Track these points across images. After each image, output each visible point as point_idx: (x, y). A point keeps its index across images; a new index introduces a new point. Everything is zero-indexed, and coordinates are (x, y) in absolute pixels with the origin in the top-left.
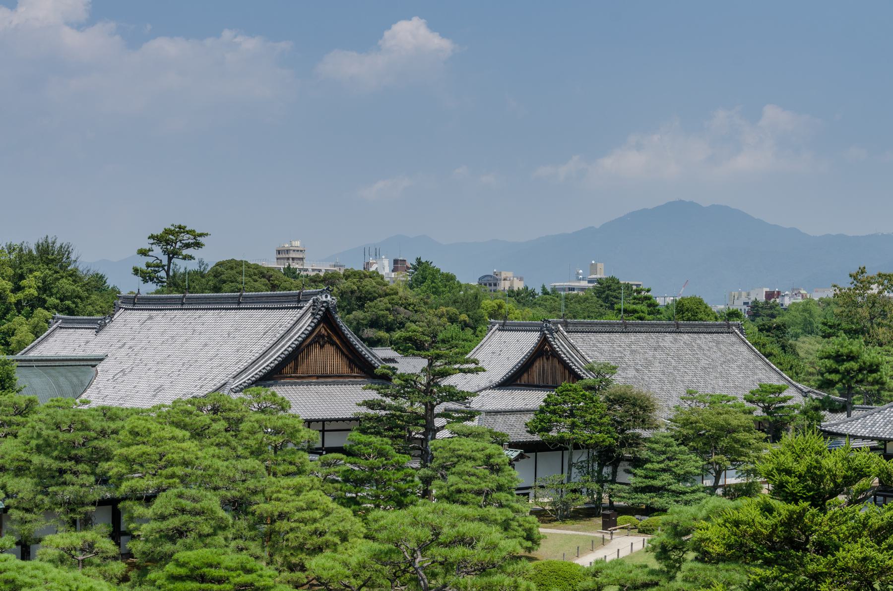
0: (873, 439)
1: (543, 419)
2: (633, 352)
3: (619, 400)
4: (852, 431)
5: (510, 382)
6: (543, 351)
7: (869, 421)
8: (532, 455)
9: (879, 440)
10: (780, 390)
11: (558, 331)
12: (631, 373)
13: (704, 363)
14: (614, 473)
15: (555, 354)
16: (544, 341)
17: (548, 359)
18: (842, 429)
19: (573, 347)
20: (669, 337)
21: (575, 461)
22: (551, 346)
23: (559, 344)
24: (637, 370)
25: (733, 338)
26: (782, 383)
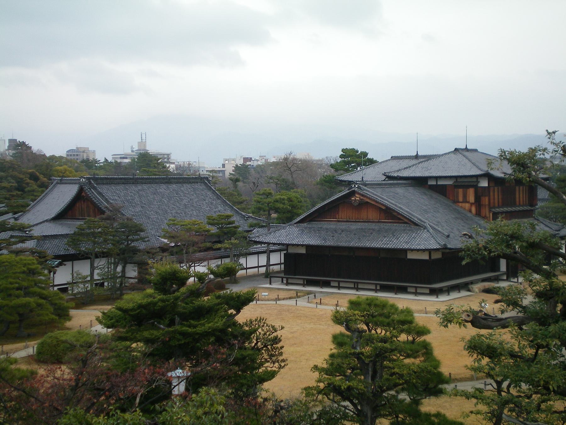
0: (279, 244)
1: (74, 239)
2: (140, 196)
3: (123, 226)
4: (267, 240)
5: (60, 217)
6: (79, 197)
7: (278, 234)
8: (69, 264)
9: (283, 244)
10: (228, 217)
11: (90, 183)
12: (138, 209)
13: (185, 201)
14: (123, 271)
15: (88, 200)
16: (81, 190)
17: (84, 202)
18: (261, 239)
19: (100, 194)
20: (164, 186)
21: (96, 265)
22: (86, 193)
23: (93, 194)
24: (142, 207)
25: (203, 186)
26: (229, 213)
